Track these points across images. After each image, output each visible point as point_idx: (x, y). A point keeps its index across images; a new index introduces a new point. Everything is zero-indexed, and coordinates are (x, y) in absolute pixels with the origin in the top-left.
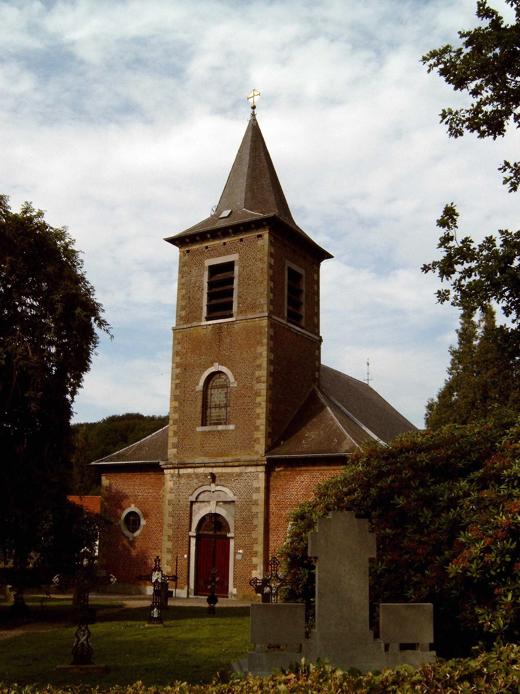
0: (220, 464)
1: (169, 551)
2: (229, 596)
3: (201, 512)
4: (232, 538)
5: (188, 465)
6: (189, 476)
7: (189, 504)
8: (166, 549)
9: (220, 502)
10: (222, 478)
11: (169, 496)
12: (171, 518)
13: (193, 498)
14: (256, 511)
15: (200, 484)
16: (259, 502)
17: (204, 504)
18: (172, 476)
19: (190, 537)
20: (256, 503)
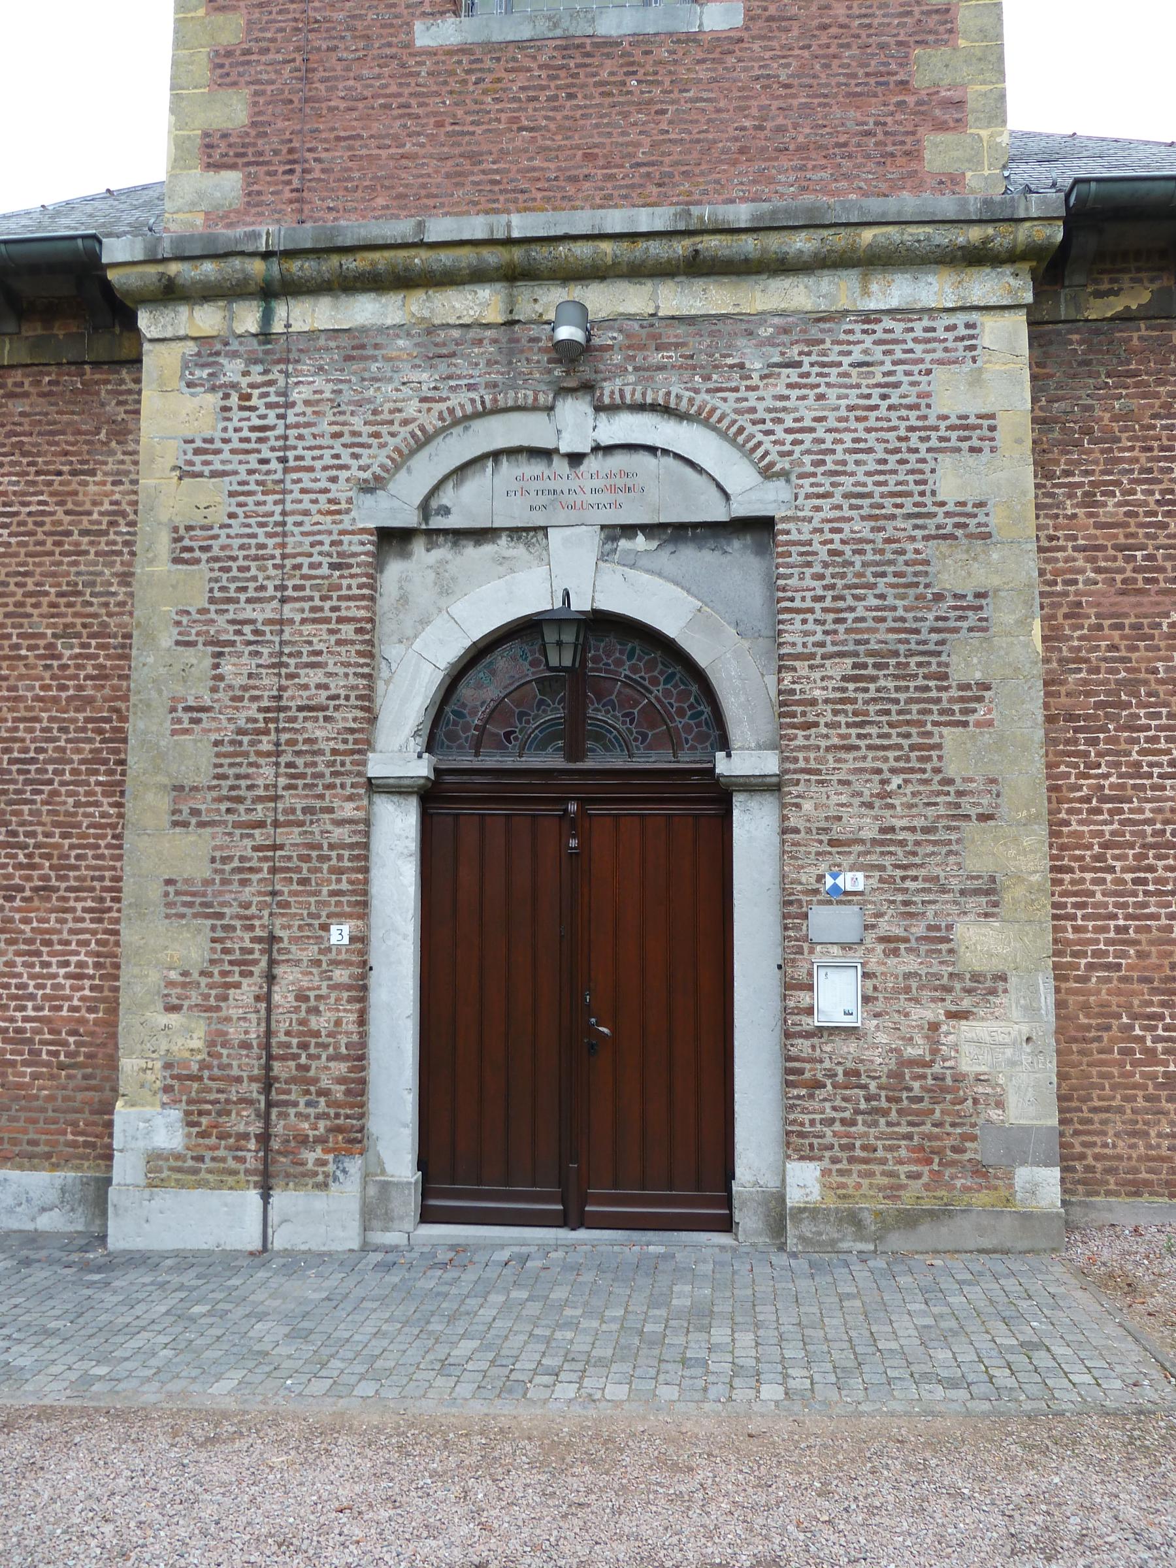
0: (656, 249)
1: (186, 900)
2: (747, 1218)
3: (459, 609)
4: (756, 786)
5: (355, 264)
6: (356, 346)
7: (360, 547)
8: (155, 891)
9: (629, 530)
10: (658, 357)
11: (168, 498)
12: (199, 659)
13: (397, 506)
14: (968, 589)
15: (461, 400)
16: (996, 519)
17: (488, 549)
18: (209, 350)
19: (374, 787)
20: (967, 527)
